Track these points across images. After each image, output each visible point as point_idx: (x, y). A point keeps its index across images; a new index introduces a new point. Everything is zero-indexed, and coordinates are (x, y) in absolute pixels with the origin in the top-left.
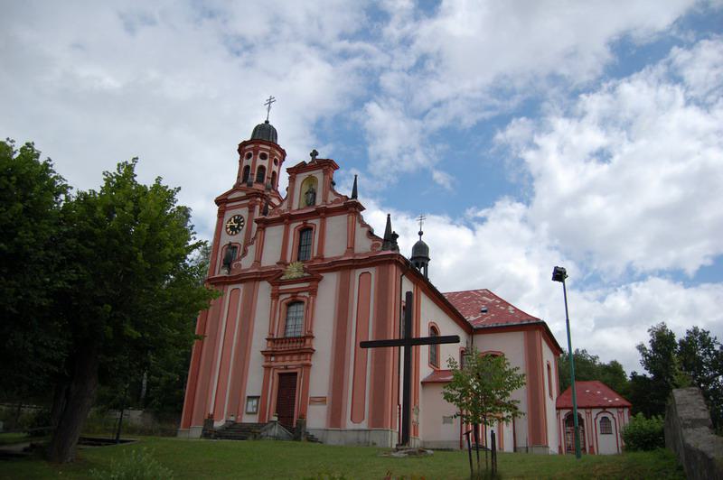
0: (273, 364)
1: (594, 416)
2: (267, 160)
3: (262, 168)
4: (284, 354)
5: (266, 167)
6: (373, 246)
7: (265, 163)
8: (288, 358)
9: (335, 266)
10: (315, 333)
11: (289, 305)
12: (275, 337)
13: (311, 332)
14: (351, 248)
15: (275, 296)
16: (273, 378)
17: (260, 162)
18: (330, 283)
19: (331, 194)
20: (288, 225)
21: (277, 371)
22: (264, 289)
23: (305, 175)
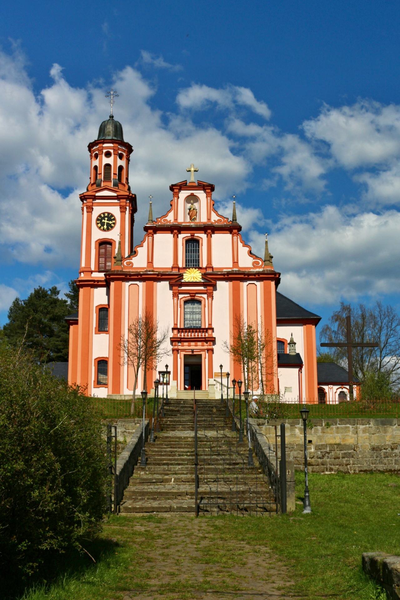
0: (180, 348)
1: (335, 390)
2: (112, 157)
3: (108, 166)
5: (112, 164)
7: (110, 161)
8: (193, 344)
9: (228, 276)
11: (186, 302)
12: (179, 327)
13: (210, 324)
14: (235, 263)
15: (175, 295)
16: (180, 358)
17: (106, 161)
18: (223, 287)
19: (213, 214)
20: (176, 237)
21: (183, 353)
22: (162, 288)
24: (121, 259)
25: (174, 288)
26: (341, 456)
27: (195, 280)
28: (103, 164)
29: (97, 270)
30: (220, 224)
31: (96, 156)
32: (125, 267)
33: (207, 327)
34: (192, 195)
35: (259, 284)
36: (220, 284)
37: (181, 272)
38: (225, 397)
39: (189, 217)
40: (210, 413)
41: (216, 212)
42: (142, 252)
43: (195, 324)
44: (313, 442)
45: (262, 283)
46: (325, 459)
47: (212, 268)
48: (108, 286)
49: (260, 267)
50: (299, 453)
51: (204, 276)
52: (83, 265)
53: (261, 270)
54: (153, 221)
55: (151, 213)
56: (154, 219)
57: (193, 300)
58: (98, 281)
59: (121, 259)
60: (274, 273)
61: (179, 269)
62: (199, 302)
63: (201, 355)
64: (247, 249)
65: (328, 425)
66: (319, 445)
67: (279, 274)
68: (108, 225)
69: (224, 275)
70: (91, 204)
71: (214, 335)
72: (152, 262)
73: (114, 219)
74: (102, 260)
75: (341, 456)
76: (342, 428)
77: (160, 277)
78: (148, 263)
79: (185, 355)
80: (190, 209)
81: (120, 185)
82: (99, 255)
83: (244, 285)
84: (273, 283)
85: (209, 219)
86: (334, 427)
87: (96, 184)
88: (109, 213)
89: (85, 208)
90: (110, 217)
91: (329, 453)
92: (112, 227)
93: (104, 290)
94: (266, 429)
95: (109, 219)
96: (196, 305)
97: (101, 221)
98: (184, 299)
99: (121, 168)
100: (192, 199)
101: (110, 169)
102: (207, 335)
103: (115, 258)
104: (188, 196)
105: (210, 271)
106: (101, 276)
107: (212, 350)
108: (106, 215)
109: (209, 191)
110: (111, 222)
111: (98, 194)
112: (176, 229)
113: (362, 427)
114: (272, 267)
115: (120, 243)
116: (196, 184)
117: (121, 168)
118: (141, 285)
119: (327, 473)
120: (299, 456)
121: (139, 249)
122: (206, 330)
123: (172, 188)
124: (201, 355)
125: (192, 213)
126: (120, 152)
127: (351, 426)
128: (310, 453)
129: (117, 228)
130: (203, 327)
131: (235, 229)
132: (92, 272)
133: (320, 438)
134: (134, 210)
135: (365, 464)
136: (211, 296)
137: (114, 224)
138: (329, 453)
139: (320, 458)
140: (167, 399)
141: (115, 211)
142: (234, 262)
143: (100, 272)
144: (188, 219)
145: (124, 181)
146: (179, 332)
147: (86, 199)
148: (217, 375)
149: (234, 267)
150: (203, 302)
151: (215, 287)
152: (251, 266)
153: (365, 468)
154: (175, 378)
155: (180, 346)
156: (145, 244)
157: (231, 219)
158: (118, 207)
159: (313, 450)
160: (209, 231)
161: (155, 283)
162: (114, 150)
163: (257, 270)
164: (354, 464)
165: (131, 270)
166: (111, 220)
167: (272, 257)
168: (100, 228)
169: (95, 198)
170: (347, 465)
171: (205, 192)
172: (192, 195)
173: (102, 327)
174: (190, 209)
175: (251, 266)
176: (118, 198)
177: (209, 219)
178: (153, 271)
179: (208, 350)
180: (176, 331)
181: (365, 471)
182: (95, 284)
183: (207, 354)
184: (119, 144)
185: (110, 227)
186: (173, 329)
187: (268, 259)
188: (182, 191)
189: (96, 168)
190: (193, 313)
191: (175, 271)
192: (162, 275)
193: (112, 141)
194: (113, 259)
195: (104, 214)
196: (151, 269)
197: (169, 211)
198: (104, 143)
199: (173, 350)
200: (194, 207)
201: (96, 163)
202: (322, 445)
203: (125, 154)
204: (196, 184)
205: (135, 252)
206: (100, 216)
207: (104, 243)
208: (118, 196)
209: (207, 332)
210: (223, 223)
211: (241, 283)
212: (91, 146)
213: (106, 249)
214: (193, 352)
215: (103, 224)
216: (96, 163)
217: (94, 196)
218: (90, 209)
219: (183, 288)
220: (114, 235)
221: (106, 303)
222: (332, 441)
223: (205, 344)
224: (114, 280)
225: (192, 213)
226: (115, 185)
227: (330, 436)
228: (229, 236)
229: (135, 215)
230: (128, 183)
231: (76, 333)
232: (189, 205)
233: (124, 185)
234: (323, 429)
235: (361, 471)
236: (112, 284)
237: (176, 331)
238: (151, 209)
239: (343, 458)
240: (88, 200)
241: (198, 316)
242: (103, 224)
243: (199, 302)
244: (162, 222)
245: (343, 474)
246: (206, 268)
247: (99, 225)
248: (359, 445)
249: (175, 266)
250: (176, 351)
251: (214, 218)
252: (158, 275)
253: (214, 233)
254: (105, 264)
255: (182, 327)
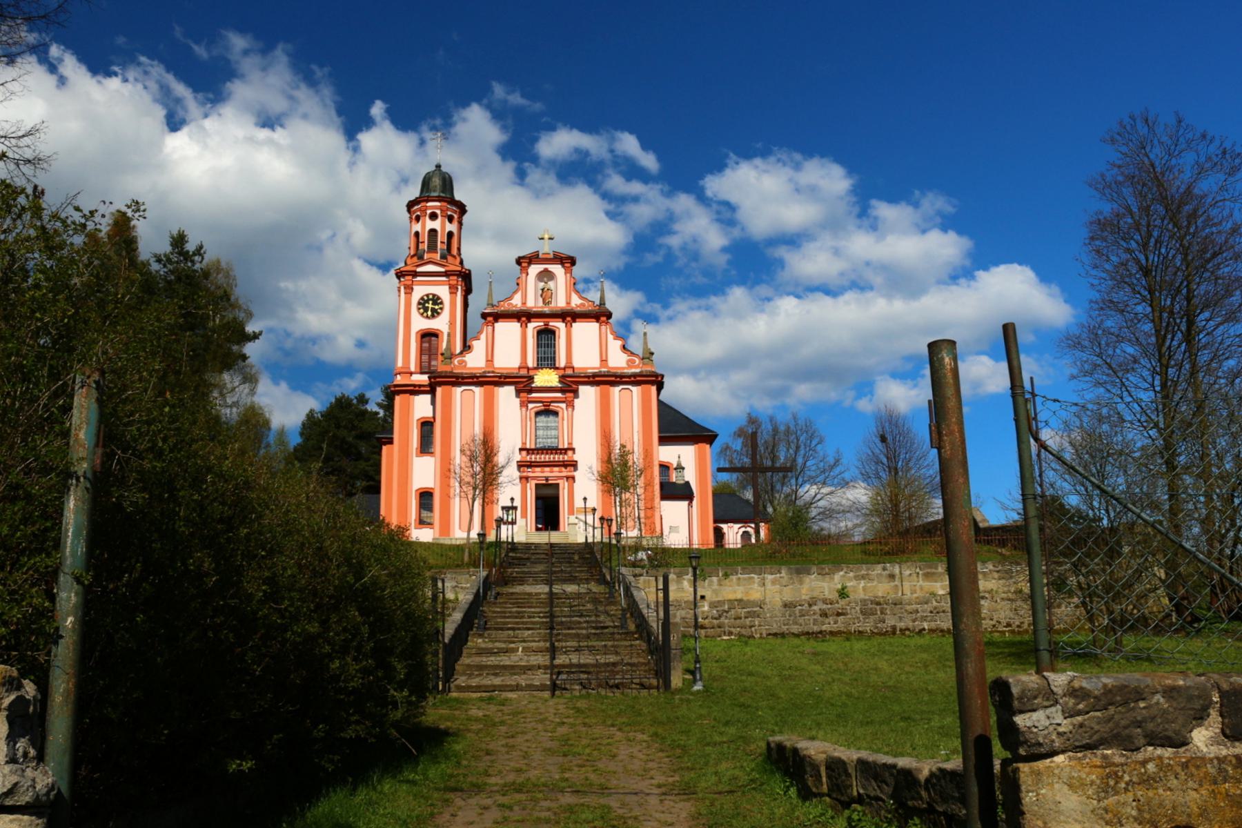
0: (530, 474)
3: (433, 232)
4: (543, 465)
5: (439, 229)
6: (628, 361)
7: (436, 225)
8: (547, 469)
10: (574, 446)
11: (538, 414)
12: (528, 447)
13: (570, 444)
14: (604, 361)
15: (524, 404)
17: (430, 225)
18: (588, 393)
21: (533, 483)
22: (506, 396)
23: (540, 268)
24: (450, 356)
25: (522, 395)
26: (743, 615)
27: (549, 385)
28: (428, 229)
29: (418, 370)
30: (583, 309)
31: (418, 219)
32: (456, 366)
33: (566, 446)
34: (546, 270)
35: (635, 389)
36: (583, 390)
37: (531, 373)
38: (590, 540)
39: (541, 300)
40: (570, 561)
41: (577, 292)
42: (479, 346)
43: (550, 443)
44: (707, 598)
45: (639, 387)
46: (722, 619)
47: (573, 368)
48: (432, 392)
49: (636, 367)
50: (688, 613)
51: (562, 378)
52: (400, 364)
53: (638, 370)
54: (493, 306)
55: (490, 295)
56: (495, 303)
57: (547, 411)
58: (420, 386)
59: (450, 356)
60: (656, 375)
61: (528, 369)
62: (556, 413)
63: (558, 484)
64: (619, 343)
65: (726, 575)
66: (715, 602)
67: (663, 376)
68: (434, 310)
69: (588, 377)
70: (410, 282)
71: (576, 458)
72: (492, 361)
73: (441, 303)
74: (425, 358)
75: (743, 615)
76: (745, 579)
77: (502, 380)
78: (487, 361)
79: (536, 485)
80: (543, 290)
81: (449, 258)
82: (421, 351)
83: (616, 391)
84: (654, 388)
85: (568, 303)
86: (734, 578)
87: (418, 255)
88: (434, 295)
89: (402, 288)
90: (436, 300)
91: (727, 612)
92: (438, 314)
93: (428, 397)
94: (644, 581)
95: (435, 303)
96: (552, 418)
97: (424, 304)
98: (536, 410)
99: (450, 234)
100: (546, 275)
101: (436, 236)
102: (566, 458)
103: (442, 354)
104: (541, 272)
105: (569, 372)
106: (424, 379)
107: (573, 478)
108: (431, 297)
109: (568, 265)
110: (436, 307)
111: (419, 269)
112: (523, 316)
113: (770, 577)
114: (652, 366)
115: (449, 335)
116: (551, 256)
117: (450, 234)
118: (478, 391)
119: (725, 638)
120: (689, 616)
121: (475, 343)
122: (565, 451)
123: (519, 261)
124: (558, 484)
125: (546, 295)
126: (449, 213)
127: (756, 576)
128: (703, 612)
129: (445, 315)
130: (560, 447)
131: (603, 316)
132: (411, 373)
133: (715, 591)
134: (468, 291)
135: (775, 625)
136: (571, 405)
137: (441, 309)
138: (727, 612)
139: (716, 619)
140: (513, 543)
141: (443, 292)
142: (602, 361)
143: (422, 373)
144: (540, 303)
145: (455, 252)
146: (528, 454)
147: (404, 276)
148: (579, 510)
149: (602, 366)
150: (560, 414)
151: (576, 393)
152: (624, 364)
153: (774, 631)
154: (524, 515)
155: (529, 472)
156: (483, 336)
157: (597, 302)
158: (447, 288)
159: (706, 608)
160: (569, 319)
161: (496, 388)
162: (442, 211)
163: (633, 370)
164: (760, 626)
165: (464, 371)
166: (438, 304)
167: (652, 354)
168: (422, 314)
169: (415, 274)
170: (751, 627)
171: (563, 267)
172: (546, 270)
173: (426, 446)
174: (543, 290)
175: (624, 364)
176: (446, 274)
177: (568, 303)
178: (493, 372)
179: (568, 478)
180: (524, 453)
181: (775, 635)
182: (415, 390)
183: (566, 484)
184: (449, 203)
185: (435, 314)
186: (521, 450)
187: (648, 355)
188: (533, 266)
189: (417, 234)
190: (547, 428)
191: (524, 372)
192: (506, 377)
193: (439, 199)
194: (440, 356)
195: (427, 295)
196: (491, 370)
197: (515, 292)
198: (427, 201)
199: (521, 478)
200: (547, 287)
201: (417, 227)
202: (719, 602)
203: (456, 216)
204: (551, 256)
205: (469, 347)
206: (422, 298)
207: (428, 336)
208: (446, 272)
209: (565, 453)
210: (588, 307)
211: (612, 388)
212: (410, 205)
213: (430, 342)
214: (547, 479)
215: (426, 310)
216: (417, 227)
217: (415, 272)
218: (409, 289)
219: (534, 395)
220: (440, 324)
221: (430, 414)
222: (732, 597)
223: (563, 469)
224: (441, 384)
225: (546, 295)
226: (443, 257)
227: (729, 589)
228: (597, 325)
229: (470, 297)
230: (459, 254)
231: (390, 455)
232: (541, 285)
233: (454, 257)
234: (719, 581)
235: (770, 634)
236: (439, 390)
237: (524, 453)
238: (491, 290)
239: (746, 617)
240: (407, 278)
241: (554, 433)
242: (426, 310)
243: (556, 413)
244: (504, 307)
245: (746, 639)
246: (564, 369)
247: (422, 311)
248: (767, 600)
249: (524, 366)
250: (523, 479)
251: (576, 301)
252: (500, 377)
253: (574, 321)
254: (429, 362)
255: (533, 447)
